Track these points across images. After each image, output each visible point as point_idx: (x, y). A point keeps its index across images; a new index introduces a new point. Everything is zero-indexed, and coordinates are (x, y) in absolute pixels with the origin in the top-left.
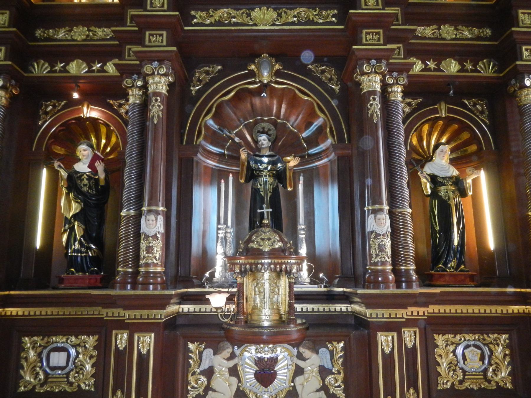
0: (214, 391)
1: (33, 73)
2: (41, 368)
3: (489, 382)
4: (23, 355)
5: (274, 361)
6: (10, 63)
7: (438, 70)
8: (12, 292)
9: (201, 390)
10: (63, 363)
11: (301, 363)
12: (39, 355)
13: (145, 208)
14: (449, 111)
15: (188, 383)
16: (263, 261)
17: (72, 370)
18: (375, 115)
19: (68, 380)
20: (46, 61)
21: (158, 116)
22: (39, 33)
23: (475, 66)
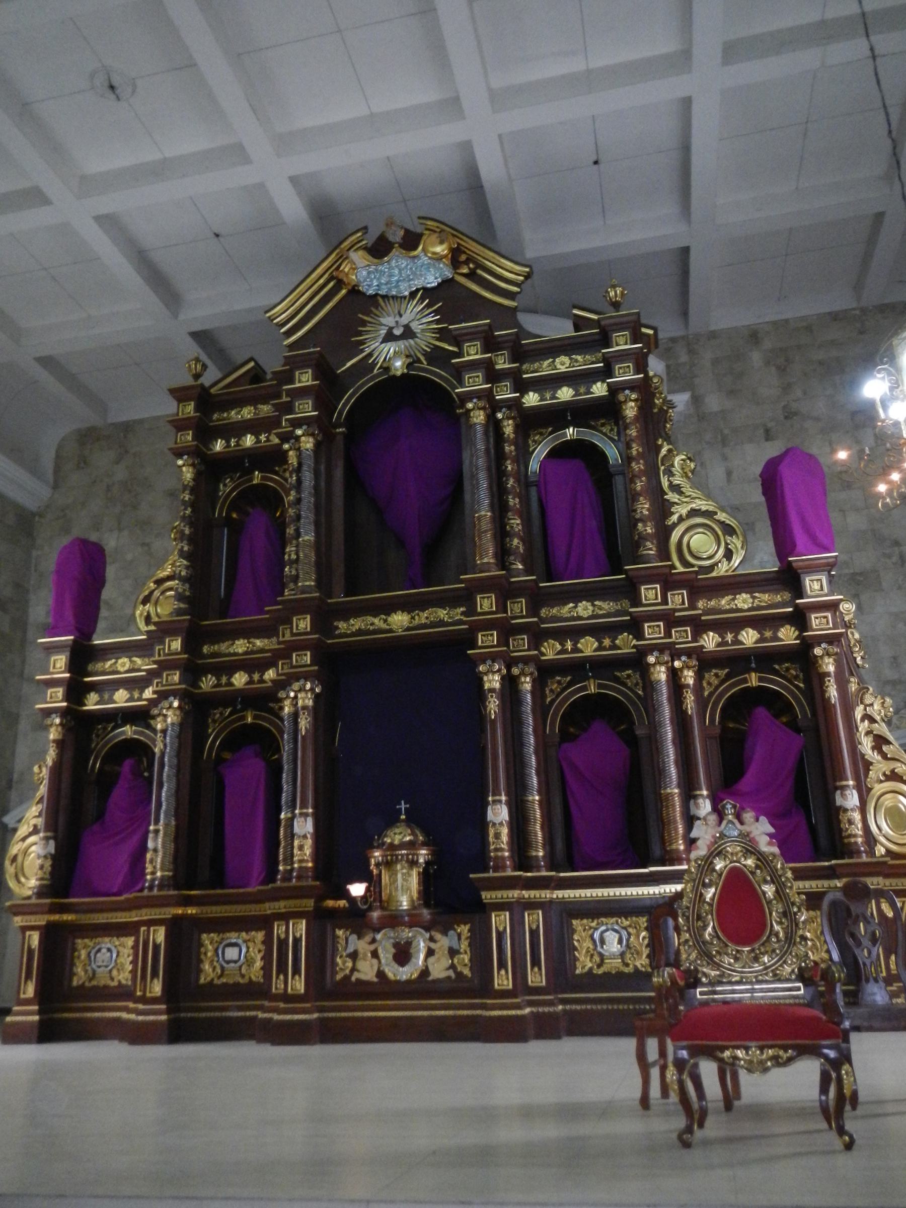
0: (358, 971)
1: (201, 688)
2: (218, 961)
3: (627, 965)
4: (203, 950)
5: (409, 944)
6: (183, 686)
7: (575, 650)
8: (192, 892)
9: (347, 972)
10: (236, 957)
11: (433, 945)
12: (216, 950)
13: (297, 811)
14: (600, 686)
15: (337, 965)
16: (397, 852)
17: (244, 963)
18: (492, 712)
19: (241, 973)
20: (212, 675)
21: (306, 728)
22: (206, 649)
23: (613, 641)
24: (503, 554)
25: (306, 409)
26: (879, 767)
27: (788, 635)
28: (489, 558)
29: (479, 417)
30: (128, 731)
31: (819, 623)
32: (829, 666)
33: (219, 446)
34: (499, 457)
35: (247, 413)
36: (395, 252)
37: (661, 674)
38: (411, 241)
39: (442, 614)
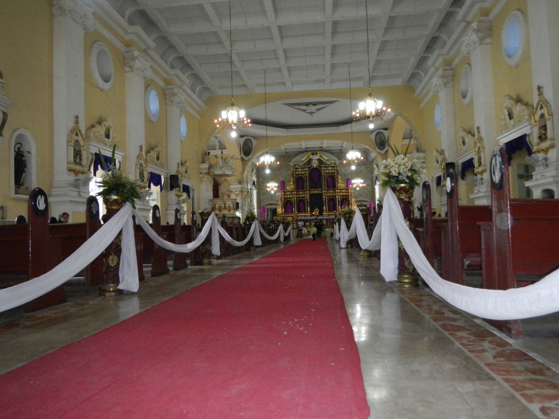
24: (325, 186)
25: (307, 171)
26: (353, 204)
27: (347, 194)
28: (324, 187)
29: (323, 174)
30: (289, 199)
31: (350, 193)
32: (350, 197)
33: (297, 173)
34: (324, 177)
35: (300, 170)
36: (315, 155)
37: (337, 197)
38: (316, 154)
39: (320, 191)
